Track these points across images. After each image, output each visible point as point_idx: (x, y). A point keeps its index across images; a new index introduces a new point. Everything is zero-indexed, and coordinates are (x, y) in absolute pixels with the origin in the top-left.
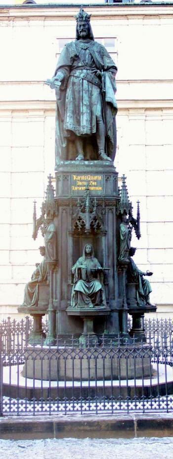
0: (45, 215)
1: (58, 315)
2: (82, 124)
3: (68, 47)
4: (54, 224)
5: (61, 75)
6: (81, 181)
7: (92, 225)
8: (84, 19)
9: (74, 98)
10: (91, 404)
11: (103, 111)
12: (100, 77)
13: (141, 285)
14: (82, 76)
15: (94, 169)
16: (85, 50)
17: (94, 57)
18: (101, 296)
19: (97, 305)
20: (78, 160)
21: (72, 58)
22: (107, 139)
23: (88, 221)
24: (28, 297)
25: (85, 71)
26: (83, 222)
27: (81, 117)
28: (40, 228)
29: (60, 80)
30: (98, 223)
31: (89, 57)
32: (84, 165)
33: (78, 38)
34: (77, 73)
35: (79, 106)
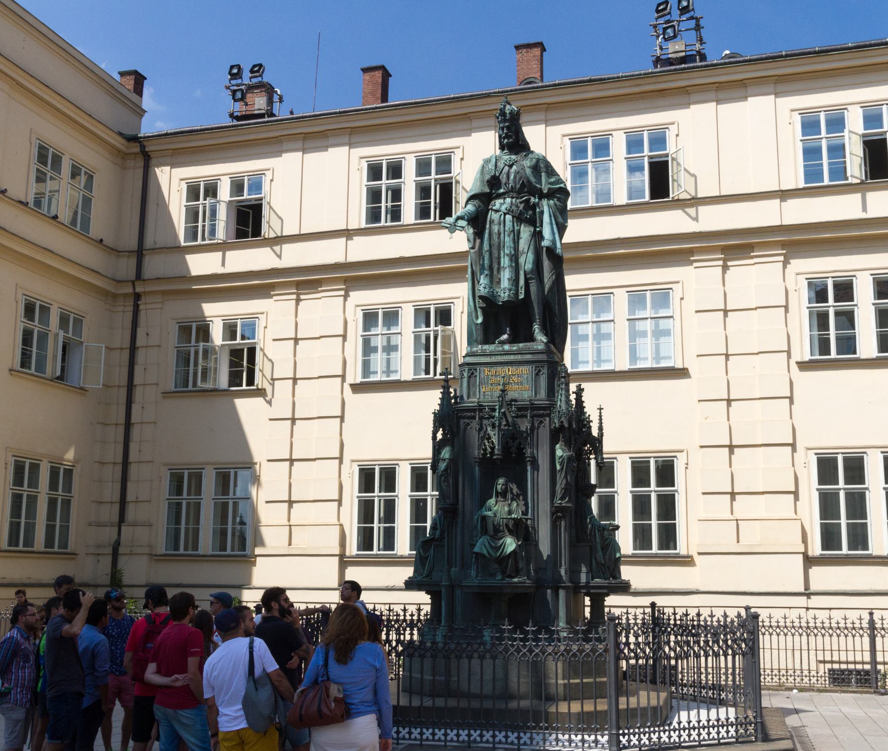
1: (458, 592)
2: (502, 286)
3: (487, 161)
4: (452, 446)
5: (470, 208)
6: (496, 376)
10: (461, 732)
13: (599, 547)
14: (503, 208)
15: (519, 357)
16: (511, 166)
18: (516, 562)
21: (488, 181)
25: (508, 200)
31: (515, 177)
32: (503, 350)
34: (497, 203)
35: (499, 258)
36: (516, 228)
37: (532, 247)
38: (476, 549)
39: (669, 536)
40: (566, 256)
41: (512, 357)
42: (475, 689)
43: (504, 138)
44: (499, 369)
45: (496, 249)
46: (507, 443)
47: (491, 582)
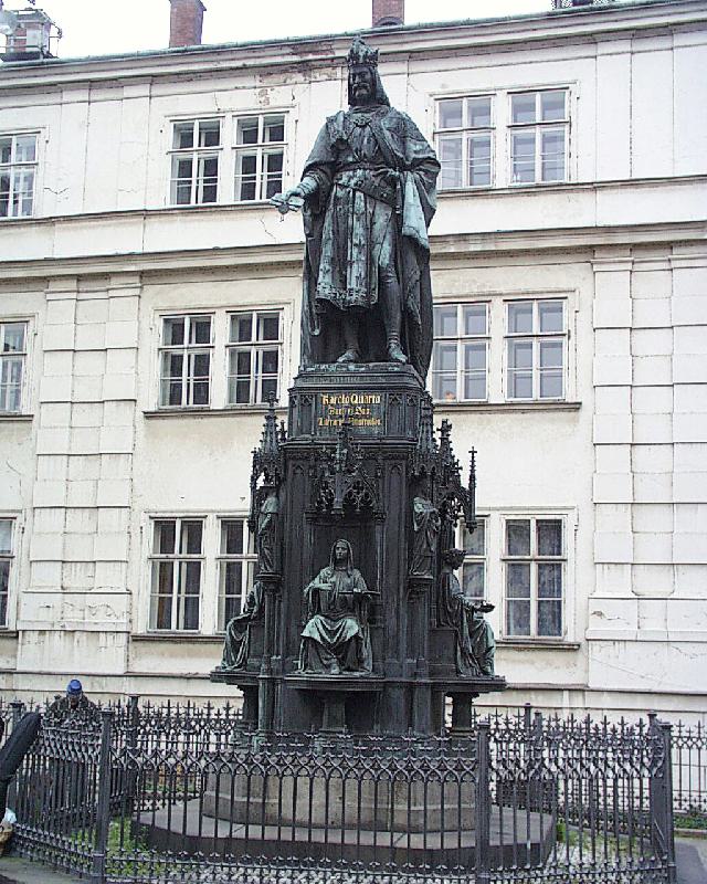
2: (348, 287)
3: (331, 121)
5: (310, 183)
8: (361, 60)
11: (396, 255)
12: (393, 182)
14: (353, 182)
16: (363, 127)
17: (380, 141)
18: (359, 651)
19: (348, 669)
21: (333, 146)
22: (407, 314)
23: (338, 492)
25: (359, 172)
26: (331, 494)
27: (349, 270)
29: (303, 194)
33: (352, 101)
37: (388, 237)
38: (306, 633)
39: (552, 615)
40: (434, 250)
42: (302, 816)
43: (356, 89)
45: (343, 237)
47: (324, 676)
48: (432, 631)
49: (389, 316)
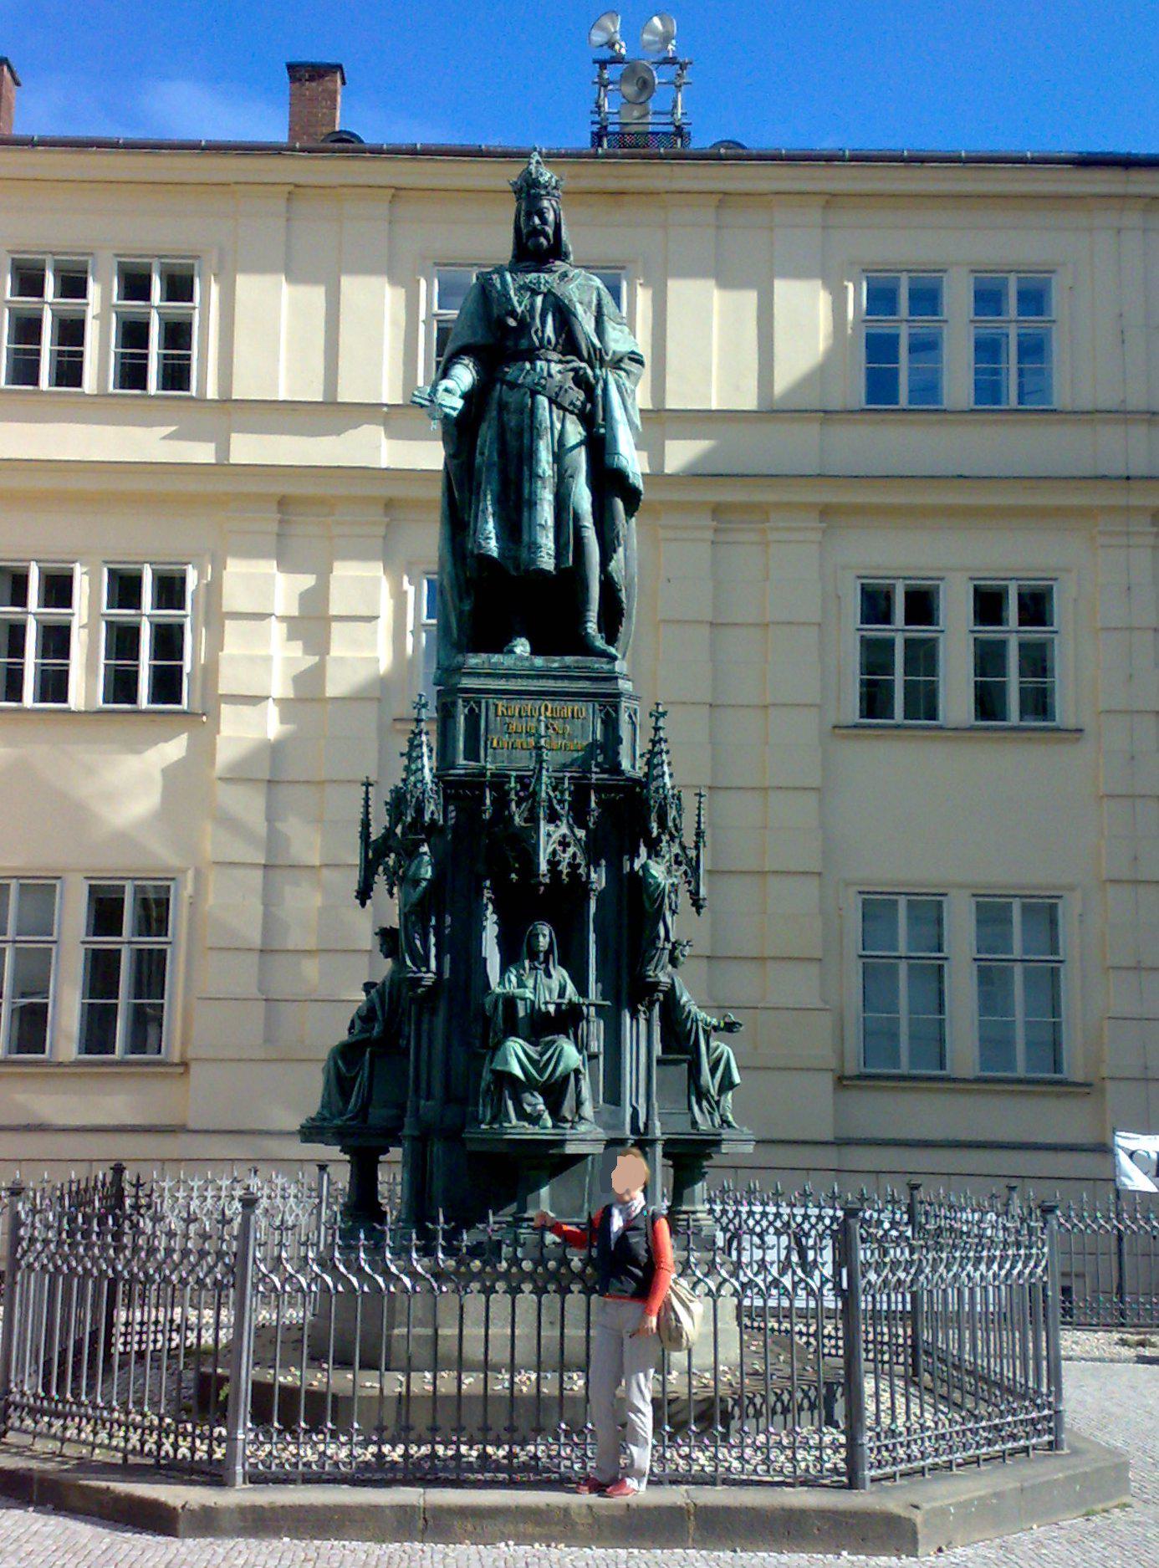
0: (399, 830)
1: (437, 1148)
2: (525, 538)
5: (464, 376)
7: (553, 864)
9: (503, 453)
20: (512, 652)
22: (609, 587)
24: (335, 1091)
27: (526, 514)
28: (381, 869)
30: (574, 856)
36: (558, 426)
41: (550, 685)
44: (529, 705)
46: (554, 853)
48: (659, 1062)
49: (585, 588)
